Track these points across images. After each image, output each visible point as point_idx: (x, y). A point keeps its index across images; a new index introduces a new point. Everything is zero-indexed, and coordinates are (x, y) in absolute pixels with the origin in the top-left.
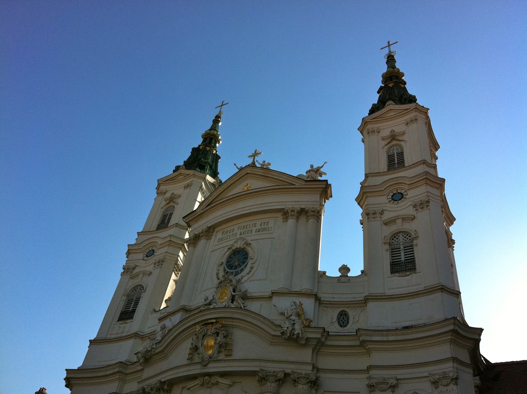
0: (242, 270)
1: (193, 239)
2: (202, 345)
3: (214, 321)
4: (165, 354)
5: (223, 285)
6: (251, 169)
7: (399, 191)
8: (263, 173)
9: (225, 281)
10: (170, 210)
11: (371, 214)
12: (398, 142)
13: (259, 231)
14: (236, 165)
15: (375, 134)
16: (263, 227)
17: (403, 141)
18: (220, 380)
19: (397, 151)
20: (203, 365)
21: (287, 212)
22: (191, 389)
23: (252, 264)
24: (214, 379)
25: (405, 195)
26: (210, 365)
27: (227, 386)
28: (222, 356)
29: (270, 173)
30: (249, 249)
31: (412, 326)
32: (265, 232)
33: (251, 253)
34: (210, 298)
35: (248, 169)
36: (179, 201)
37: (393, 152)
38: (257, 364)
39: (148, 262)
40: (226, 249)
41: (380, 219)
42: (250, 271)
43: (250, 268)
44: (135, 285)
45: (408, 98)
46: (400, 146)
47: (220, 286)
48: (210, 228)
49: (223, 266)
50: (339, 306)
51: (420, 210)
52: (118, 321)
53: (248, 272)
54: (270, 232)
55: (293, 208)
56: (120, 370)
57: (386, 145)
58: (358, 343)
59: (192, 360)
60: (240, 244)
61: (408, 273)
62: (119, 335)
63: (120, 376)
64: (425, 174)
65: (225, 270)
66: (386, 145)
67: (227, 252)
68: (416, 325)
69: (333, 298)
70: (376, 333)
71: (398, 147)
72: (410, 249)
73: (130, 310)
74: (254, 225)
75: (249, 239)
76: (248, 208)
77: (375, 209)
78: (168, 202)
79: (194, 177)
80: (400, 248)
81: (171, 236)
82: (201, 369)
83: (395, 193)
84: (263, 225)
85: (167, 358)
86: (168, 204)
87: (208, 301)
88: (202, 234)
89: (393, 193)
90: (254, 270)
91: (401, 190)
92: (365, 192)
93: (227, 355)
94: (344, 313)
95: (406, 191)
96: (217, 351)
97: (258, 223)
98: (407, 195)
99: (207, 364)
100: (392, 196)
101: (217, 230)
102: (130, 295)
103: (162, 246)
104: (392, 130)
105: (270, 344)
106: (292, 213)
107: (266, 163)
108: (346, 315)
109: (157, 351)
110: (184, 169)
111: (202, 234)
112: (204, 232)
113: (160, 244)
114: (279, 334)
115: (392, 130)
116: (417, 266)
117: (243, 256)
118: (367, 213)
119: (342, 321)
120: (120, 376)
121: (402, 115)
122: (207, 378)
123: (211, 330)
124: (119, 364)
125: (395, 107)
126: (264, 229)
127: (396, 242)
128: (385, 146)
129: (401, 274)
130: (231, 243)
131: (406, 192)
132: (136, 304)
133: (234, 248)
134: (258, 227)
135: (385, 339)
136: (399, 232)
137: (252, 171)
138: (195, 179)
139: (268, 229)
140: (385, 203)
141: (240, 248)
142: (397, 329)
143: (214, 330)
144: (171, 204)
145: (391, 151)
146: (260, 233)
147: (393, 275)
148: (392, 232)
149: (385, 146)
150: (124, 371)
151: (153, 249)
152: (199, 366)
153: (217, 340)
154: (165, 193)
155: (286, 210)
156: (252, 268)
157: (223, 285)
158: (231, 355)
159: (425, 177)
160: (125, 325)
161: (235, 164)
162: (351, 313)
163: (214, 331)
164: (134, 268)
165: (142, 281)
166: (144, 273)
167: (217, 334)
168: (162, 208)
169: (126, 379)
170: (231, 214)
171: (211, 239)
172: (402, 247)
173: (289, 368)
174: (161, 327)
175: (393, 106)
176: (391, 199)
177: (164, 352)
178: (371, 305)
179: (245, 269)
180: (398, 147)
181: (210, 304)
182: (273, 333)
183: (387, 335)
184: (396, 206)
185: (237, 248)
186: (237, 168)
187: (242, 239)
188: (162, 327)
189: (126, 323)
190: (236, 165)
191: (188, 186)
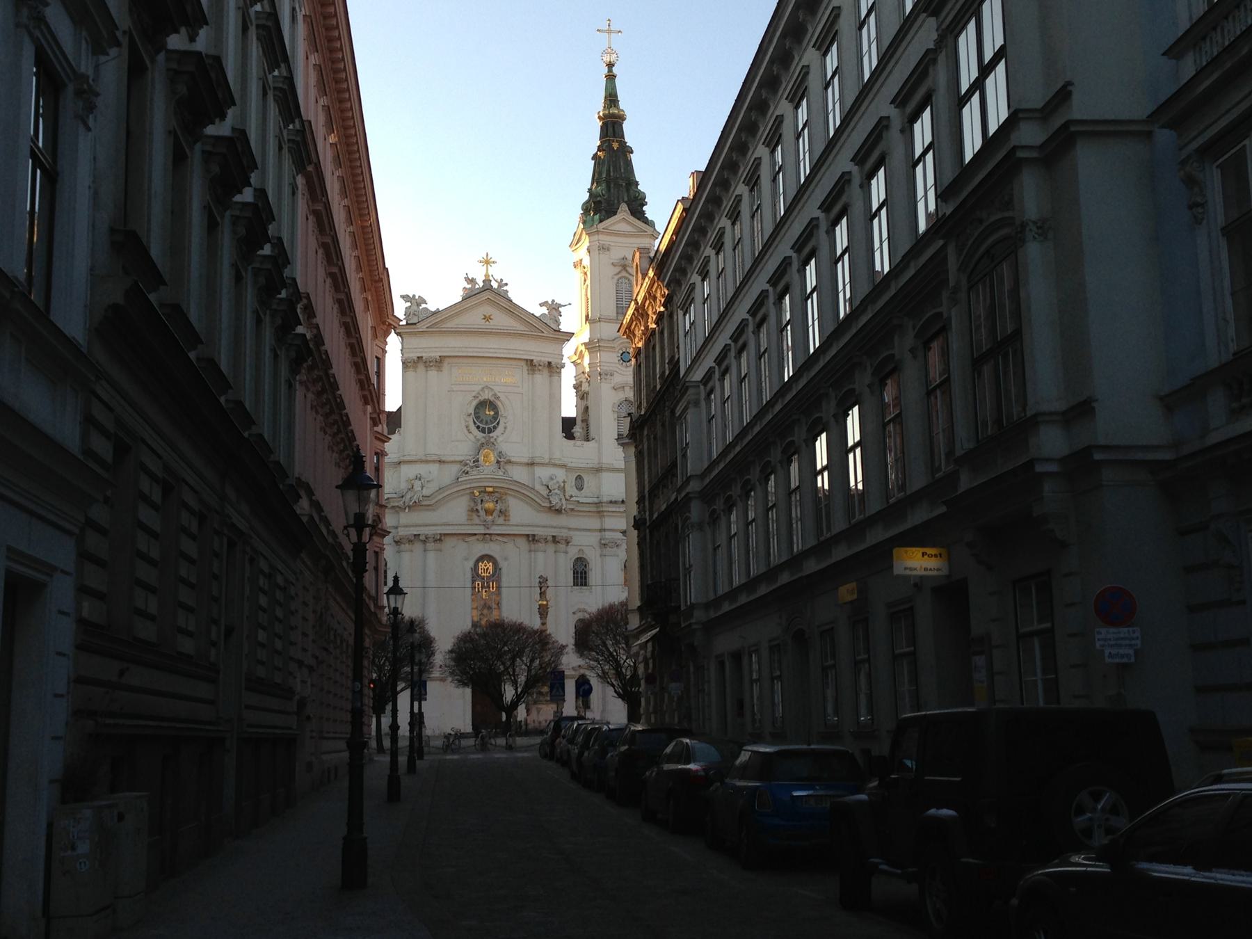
0: (495, 428)
2: (482, 509)
3: (491, 489)
12: (627, 275)
18: (499, 538)
24: (494, 538)
26: (494, 527)
28: (501, 520)
30: (499, 404)
33: (502, 411)
42: (504, 431)
45: (640, 199)
55: (540, 361)
57: (616, 275)
60: (487, 395)
65: (475, 423)
66: (616, 275)
71: (626, 281)
75: (496, 389)
76: (493, 351)
88: (431, 364)
100: (622, 355)
106: (540, 368)
107: (503, 282)
114: (548, 505)
122: (487, 536)
130: (478, 388)
133: (481, 398)
137: (495, 298)
140: (616, 363)
152: (482, 527)
158: (509, 520)
162: (585, 477)
167: (497, 501)
173: (554, 532)
178: (605, 475)
182: (543, 505)
184: (624, 369)
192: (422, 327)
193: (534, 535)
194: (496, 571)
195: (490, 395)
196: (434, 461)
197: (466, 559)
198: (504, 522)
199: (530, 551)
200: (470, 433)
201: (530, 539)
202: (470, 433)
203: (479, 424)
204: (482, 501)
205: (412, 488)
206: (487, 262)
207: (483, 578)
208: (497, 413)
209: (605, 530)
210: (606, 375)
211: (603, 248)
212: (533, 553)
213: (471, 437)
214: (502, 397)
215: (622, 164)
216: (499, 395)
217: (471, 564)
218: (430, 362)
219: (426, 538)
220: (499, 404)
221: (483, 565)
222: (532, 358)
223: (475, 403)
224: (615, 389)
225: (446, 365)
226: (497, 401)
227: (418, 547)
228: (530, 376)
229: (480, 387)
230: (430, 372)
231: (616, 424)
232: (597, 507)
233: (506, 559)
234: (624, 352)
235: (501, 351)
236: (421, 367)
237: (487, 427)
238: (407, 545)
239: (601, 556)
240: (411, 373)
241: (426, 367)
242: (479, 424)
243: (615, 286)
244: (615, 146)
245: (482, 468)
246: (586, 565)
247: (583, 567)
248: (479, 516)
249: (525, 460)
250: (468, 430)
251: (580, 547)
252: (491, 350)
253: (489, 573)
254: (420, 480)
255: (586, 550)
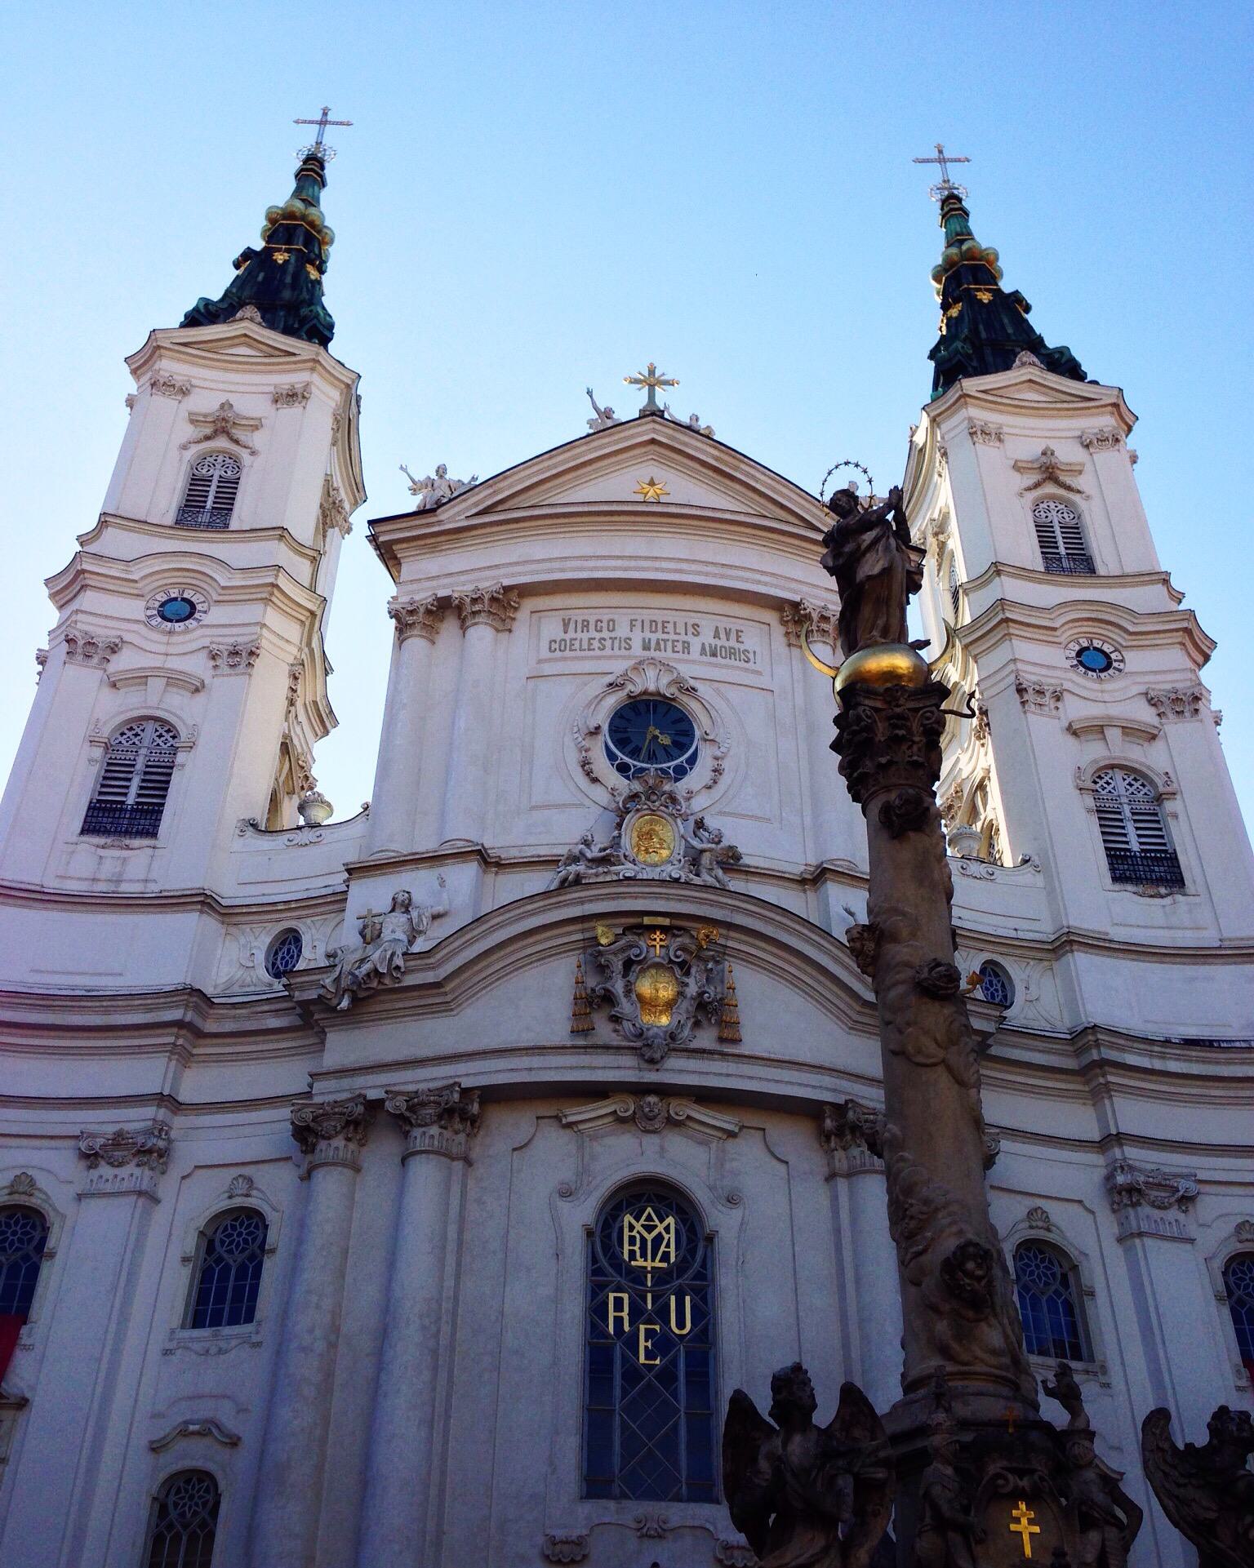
0: (681, 772)
1: (429, 612)
2: (628, 991)
4: (446, 994)
5: (645, 807)
6: (670, 432)
7: (1097, 644)
8: (717, 459)
9: (655, 798)
10: (218, 466)
11: (1030, 690)
13: (714, 655)
14: (591, 397)
15: (991, 444)
16: (722, 642)
17: (1079, 492)
19: (1062, 521)
20: (651, 1061)
21: (808, 617)
22: (581, 1127)
23: (717, 758)
25: (1115, 661)
26: (674, 1062)
27: (719, 1134)
28: (706, 1038)
29: (743, 466)
31: (1211, 1041)
32: (732, 662)
33: (702, 723)
34: (601, 840)
35: (657, 427)
36: (257, 439)
37: (1047, 517)
38: (827, 1080)
39: (174, 639)
40: (598, 685)
41: (1054, 712)
43: (714, 771)
44: (136, 714)
46: (1069, 504)
47: (638, 810)
48: (507, 589)
49: (601, 738)
50: (981, 946)
51: (1171, 715)
52: (83, 832)
53: (707, 780)
54: (750, 665)
56: (188, 1019)
57: (1029, 489)
58: (1070, 1063)
59: (586, 1035)
60: (652, 681)
61: (1163, 891)
62: (101, 887)
63: (177, 1037)
64: (1185, 617)
65: (611, 756)
66: (1029, 489)
67: (605, 695)
68: (1223, 1041)
69: (960, 918)
70: (1135, 1045)
71: (1060, 507)
72: (1152, 817)
73: (131, 800)
74: (691, 630)
75: (686, 671)
76: (672, 565)
77: (1043, 680)
78: (208, 431)
79: (313, 369)
80: (1120, 813)
81: (278, 571)
82: (640, 1070)
83: (1085, 644)
84: (722, 635)
85: (452, 1010)
86: (208, 438)
87: (593, 853)
88: (477, 608)
89: (1079, 643)
90: (725, 780)
91: (1101, 643)
92: (1007, 620)
93: (722, 1040)
94: (992, 970)
95: (1116, 650)
96: (692, 1020)
97: (707, 626)
98: (1122, 661)
99: (662, 1058)
100: (1079, 654)
101: (529, 604)
102: (111, 746)
103: (231, 596)
104: (1048, 448)
105: (851, 1028)
106: (824, 626)
108: (997, 975)
109: (409, 980)
110: (260, 324)
111: (477, 608)
112: (486, 601)
113: (224, 588)
115: (1048, 448)
116: (1186, 875)
117: (675, 722)
118: (1024, 686)
119: (997, 990)
120: (177, 1037)
121: (1068, 409)
122: (652, 1099)
123: (657, 946)
124: (186, 997)
125: (1045, 379)
126: (731, 653)
127: (1103, 792)
128: (1026, 490)
129: (1140, 889)
131: (1117, 653)
132: (163, 787)
134: (707, 637)
135: (1158, 1065)
136: (1112, 767)
138: (315, 378)
139: (743, 657)
141: (659, 694)
142: (1167, 1042)
143: (679, 953)
144: (222, 443)
145: (1044, 515)
146: (719, 660)
147: (1117, 887)
148: (1095, 761)
149: (1026, 490)
150: (198, 1022)
151: (185, 596)
152: (628, 1060)
153: (687, 985)
154: (184, 392)
155: (808, 611)
156: (717, 771)
157: (645, 807)
158: (737, 1041)
159: (1185, 624)
160: (125, 853)
161: (590, 393)
162: (1017, 971)
163: (678, 957)
164: (114, 649)
165: (162, 706)
166: (175, 680)
167: (686, 968)
168: (184, 447)
169: (195, 1051)
170: (626, 569)
171: (510, 631)
172: (1127, 809)
174: (394, 899)
175: (1039, 373)
176: (1075, 662)
177: (442, 990)
178: (1081, 960)
179: (691, 769)
180: (1060, 507)
181: (604, 861)
183: (1162, 1056)
185: (645, 692)
186: (596, 409)
187: (659, 667)
188: (400, 898)
189: (128, 848)
190: (591, 397)
191: (293, 396)
192: (451, 517)
193: (840, 1109)
194: (692, 1251)
195: (665, 680)
196: (460, 856)
197: (566, 1193)
198: (718, 1047)
199: (831, 1177)
200: (595, 780)
201: (829, 1123)
202: (595, 780)
203: (627, 760)
204: (628, 964)
205: (379, 936)
206: (652, 381)
207: (638, 1276)
208: (689, 733)
209: (1120, 1138)
210: (1040, 693)
211: (983, 432)
212: (842, 1185)
213: (600, 794)
214: (703, 689)
215: (1006, 321)
216: (692, 683)
217: (583, 1213)
218: (474, 601)
219: (409, 1109)
220: (694, 706)
221: (638, 1226)
222: (797, 599)
223: (613, 701)
224: (1075, 733)
225: (523, 615)
226: (685, 699)
227: (381, 1152)
228: (795, 651)
229: (632, 663)
230: (473, 632)
231: (1097, 830)
232: (1078, 1053)
233: (732, 1200)
234: (1087, 649)
235: (694, 567)
236: (449, 628)
237: (652, 767)
238: (339, 1142)
239: (1120, 1240)
240: (416, 643)
241: (463, 621)
242: (627, 760)
243: (1031, 514)
244: (985, 297)
245: (631, 865)
246: (1064, 1276)
247: (1056, 1286)
248: (615, 1019)
249: (796, 870)
250: (588, 774)
251: (1040, 1202)
252: (664, 565)
253: (666, 1257)
254: (407, 911)
255: (1054, 1209)
